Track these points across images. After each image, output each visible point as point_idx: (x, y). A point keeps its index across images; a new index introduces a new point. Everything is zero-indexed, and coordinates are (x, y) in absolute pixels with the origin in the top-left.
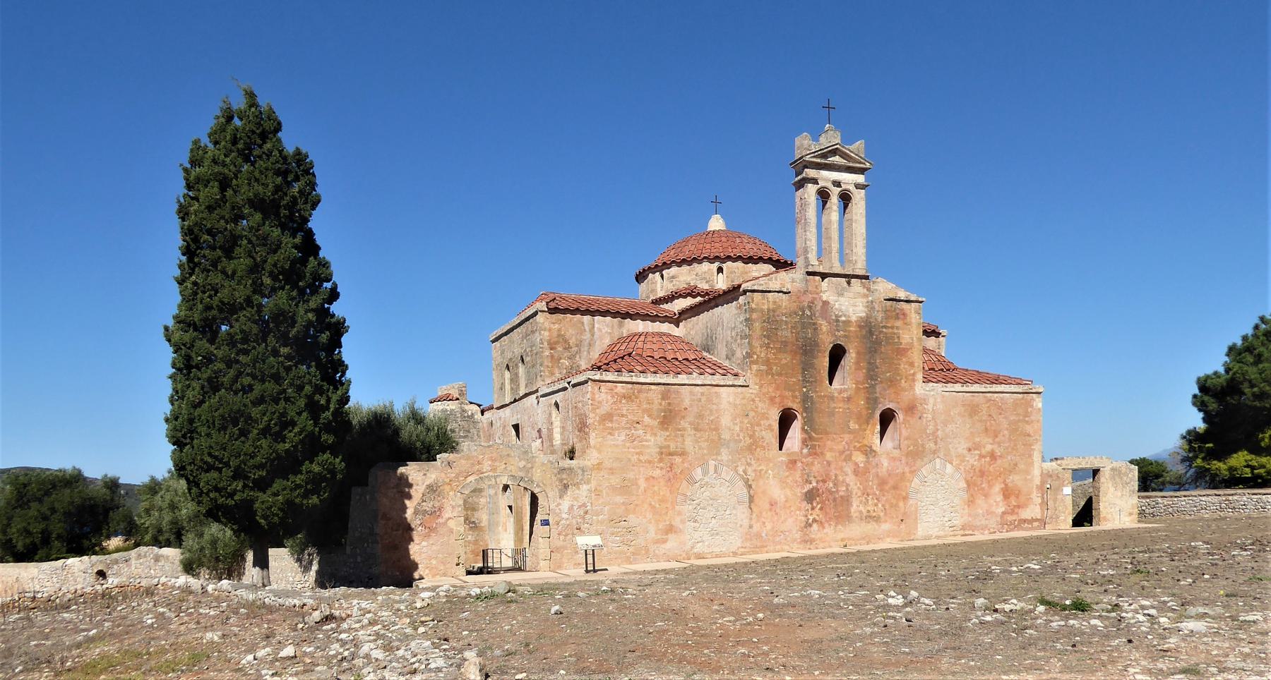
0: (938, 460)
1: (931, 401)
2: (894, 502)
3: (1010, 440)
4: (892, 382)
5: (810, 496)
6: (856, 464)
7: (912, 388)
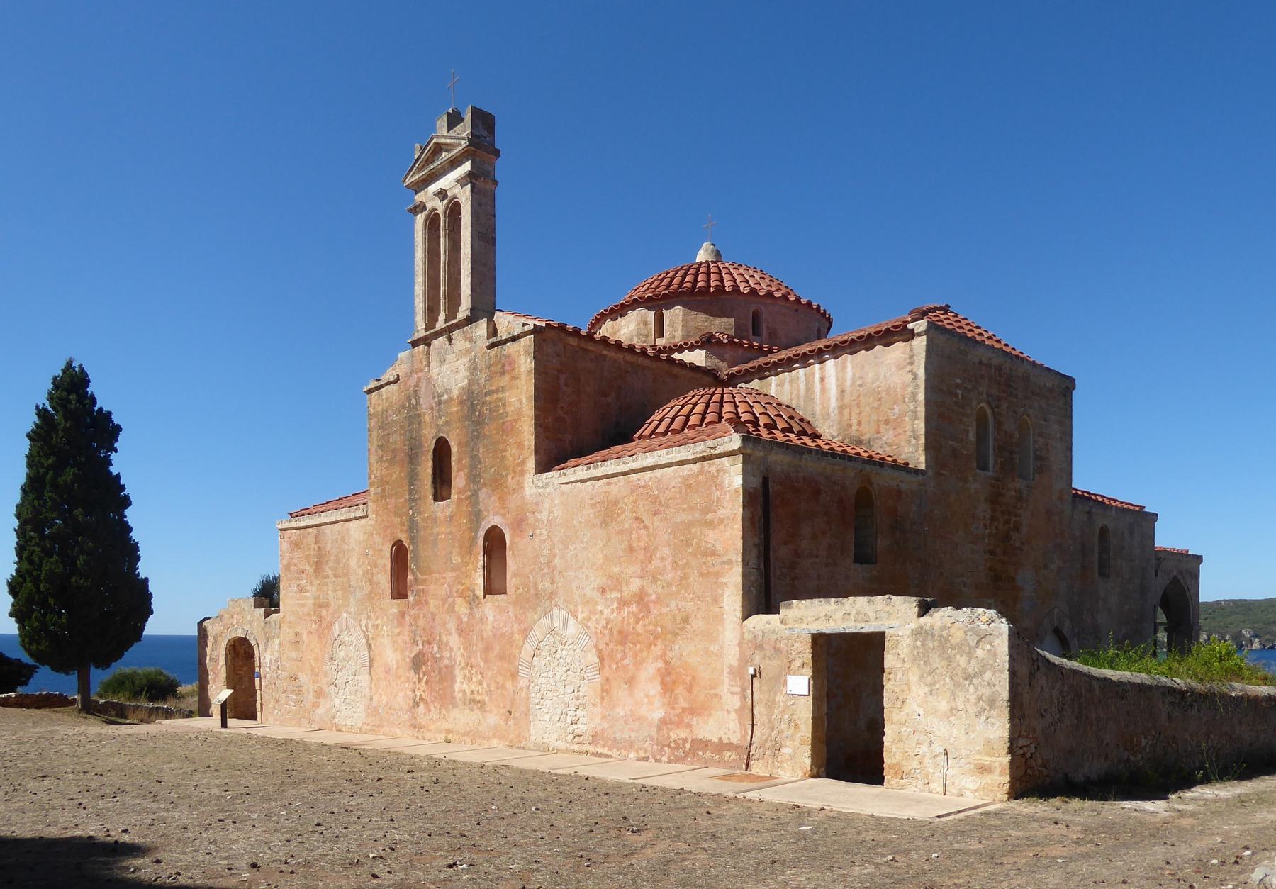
0: (556, 611)
1: (546, 506)
2: (500, 679)
3: (675, 565)
4: (497, 484)
5: (418, 663)
6: (459, 618)
7: (520, 486)
